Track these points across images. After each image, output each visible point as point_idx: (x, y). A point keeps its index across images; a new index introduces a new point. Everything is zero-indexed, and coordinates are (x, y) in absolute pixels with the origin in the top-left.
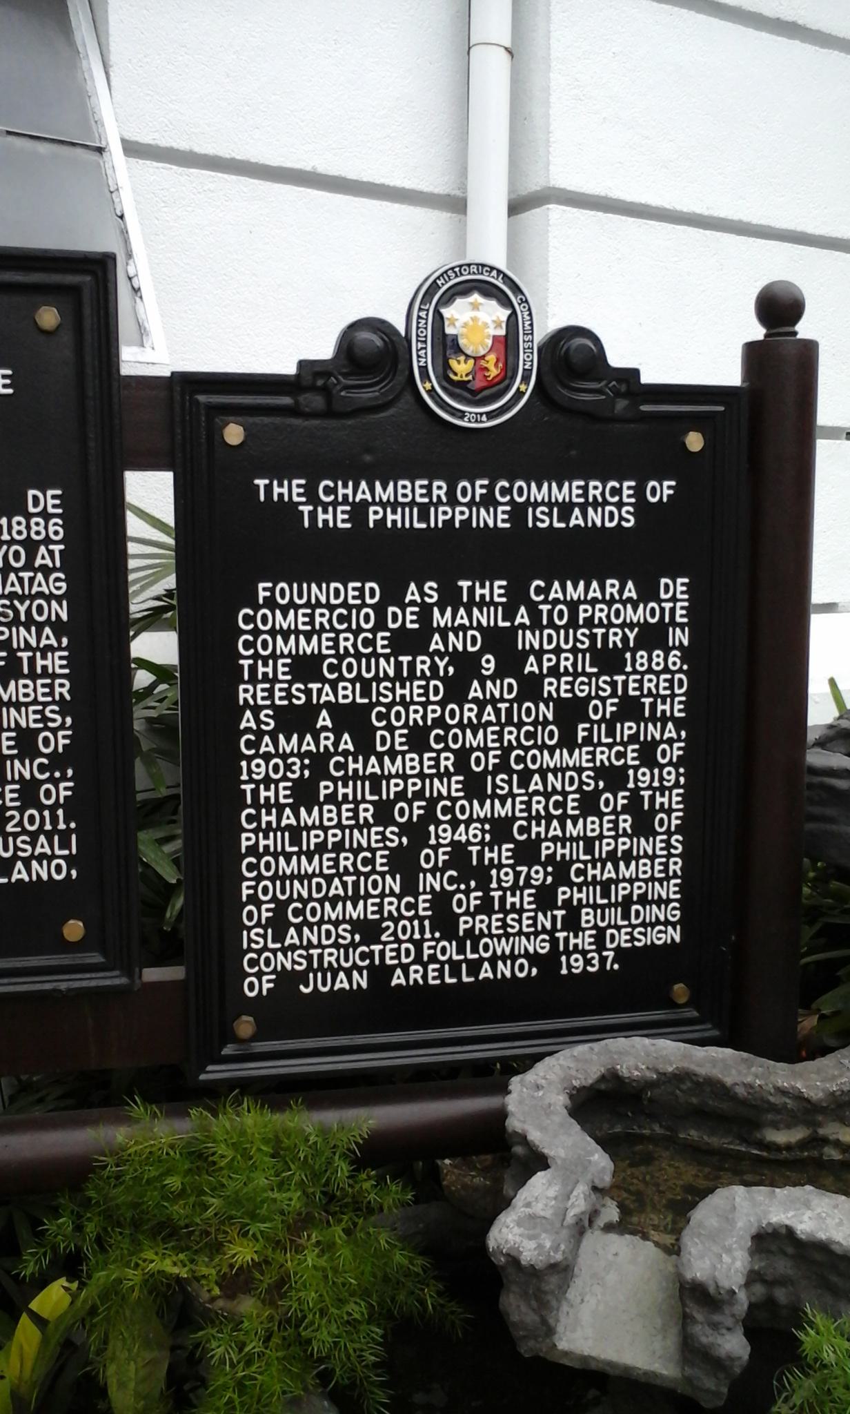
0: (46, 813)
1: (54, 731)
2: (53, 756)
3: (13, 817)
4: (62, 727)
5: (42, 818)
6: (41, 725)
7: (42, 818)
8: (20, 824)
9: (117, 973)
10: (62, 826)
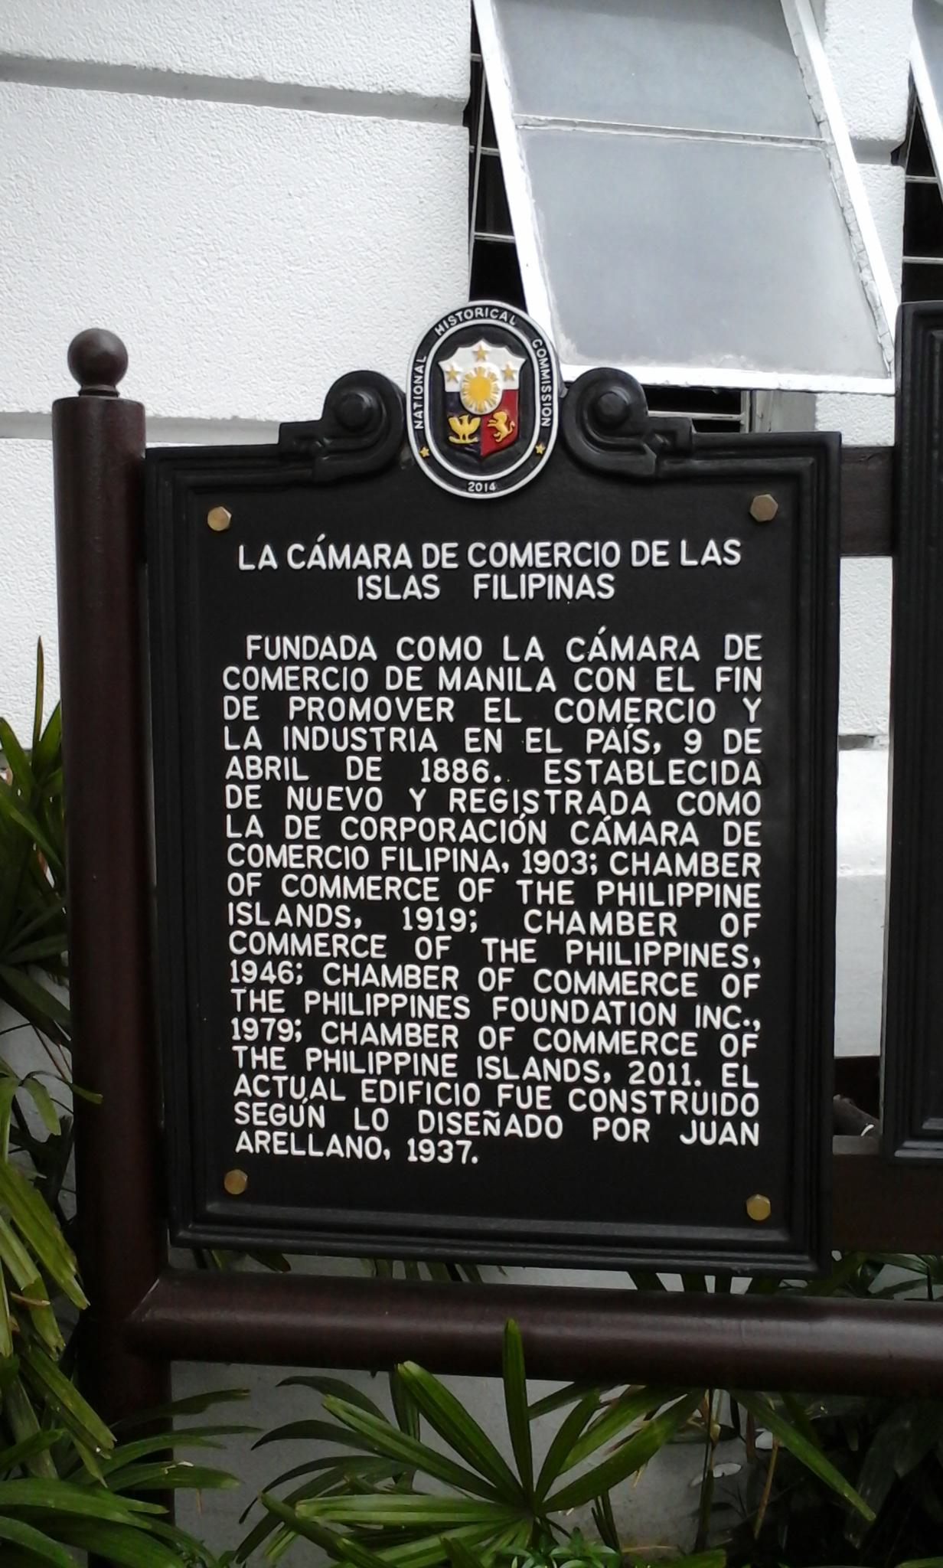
0: (672, 1066)
1: (741, 973)
2: (739, 1000)
3: (636, 1068)
4: (751, 968)
5: (667, 1071)
6: (725, 965)
7: (667, 1071)
8: (645, 1076)
9: (806, 1258)
10: (687, 1083)
